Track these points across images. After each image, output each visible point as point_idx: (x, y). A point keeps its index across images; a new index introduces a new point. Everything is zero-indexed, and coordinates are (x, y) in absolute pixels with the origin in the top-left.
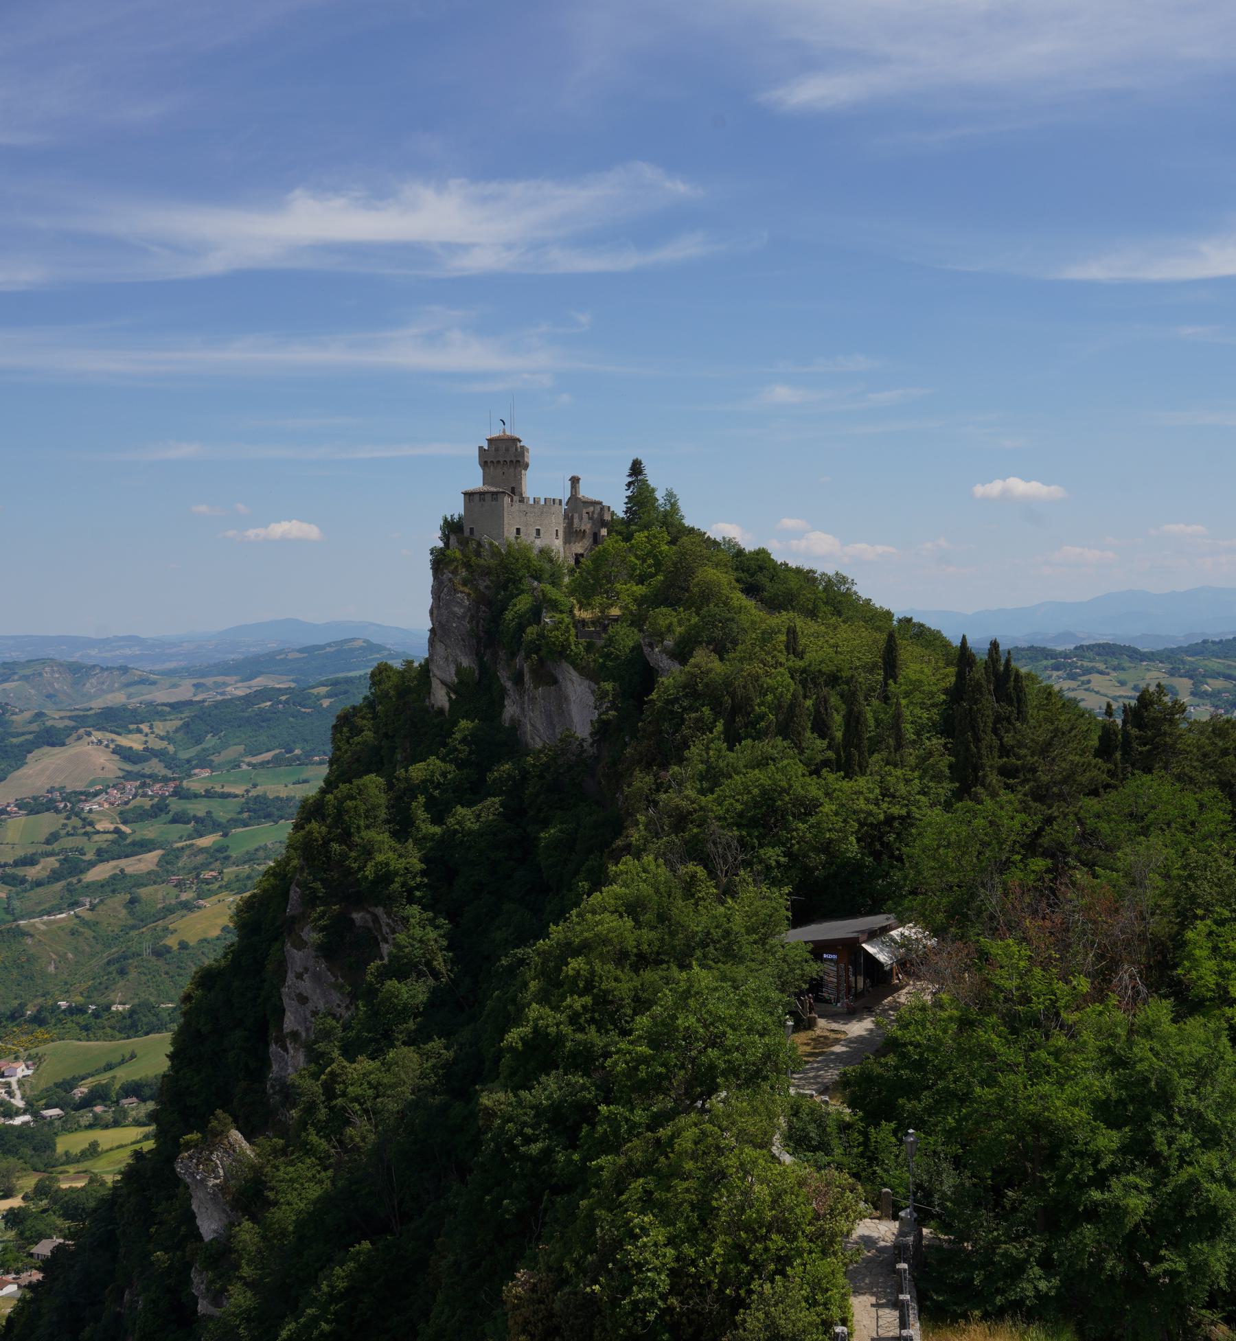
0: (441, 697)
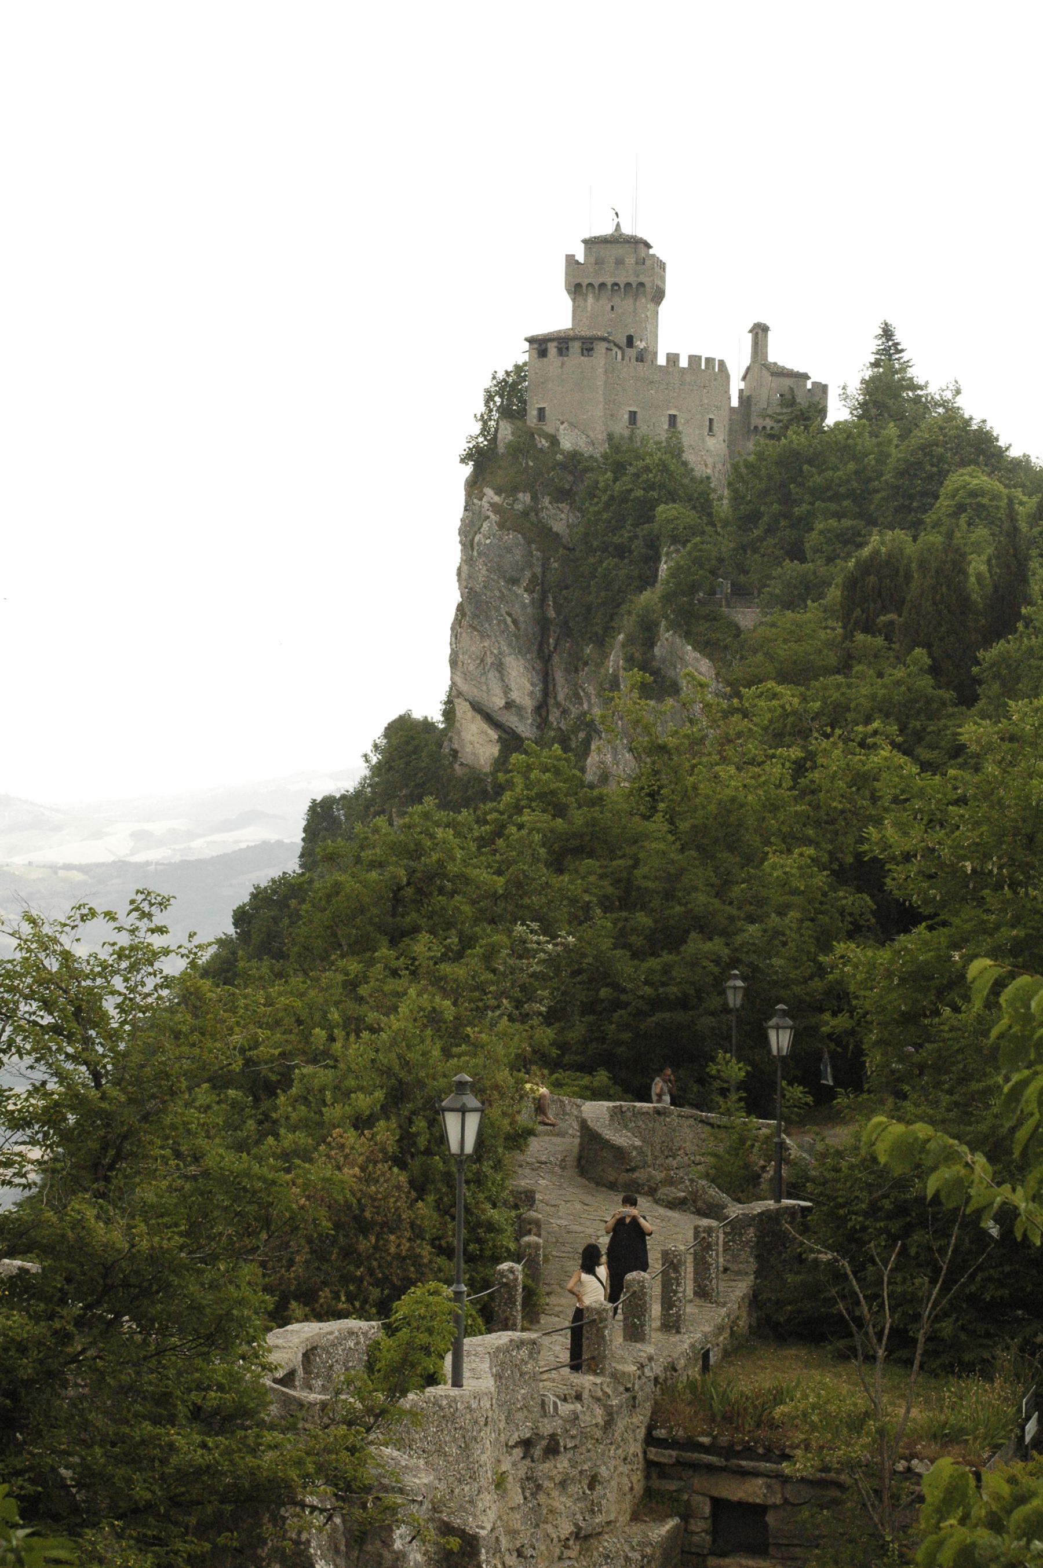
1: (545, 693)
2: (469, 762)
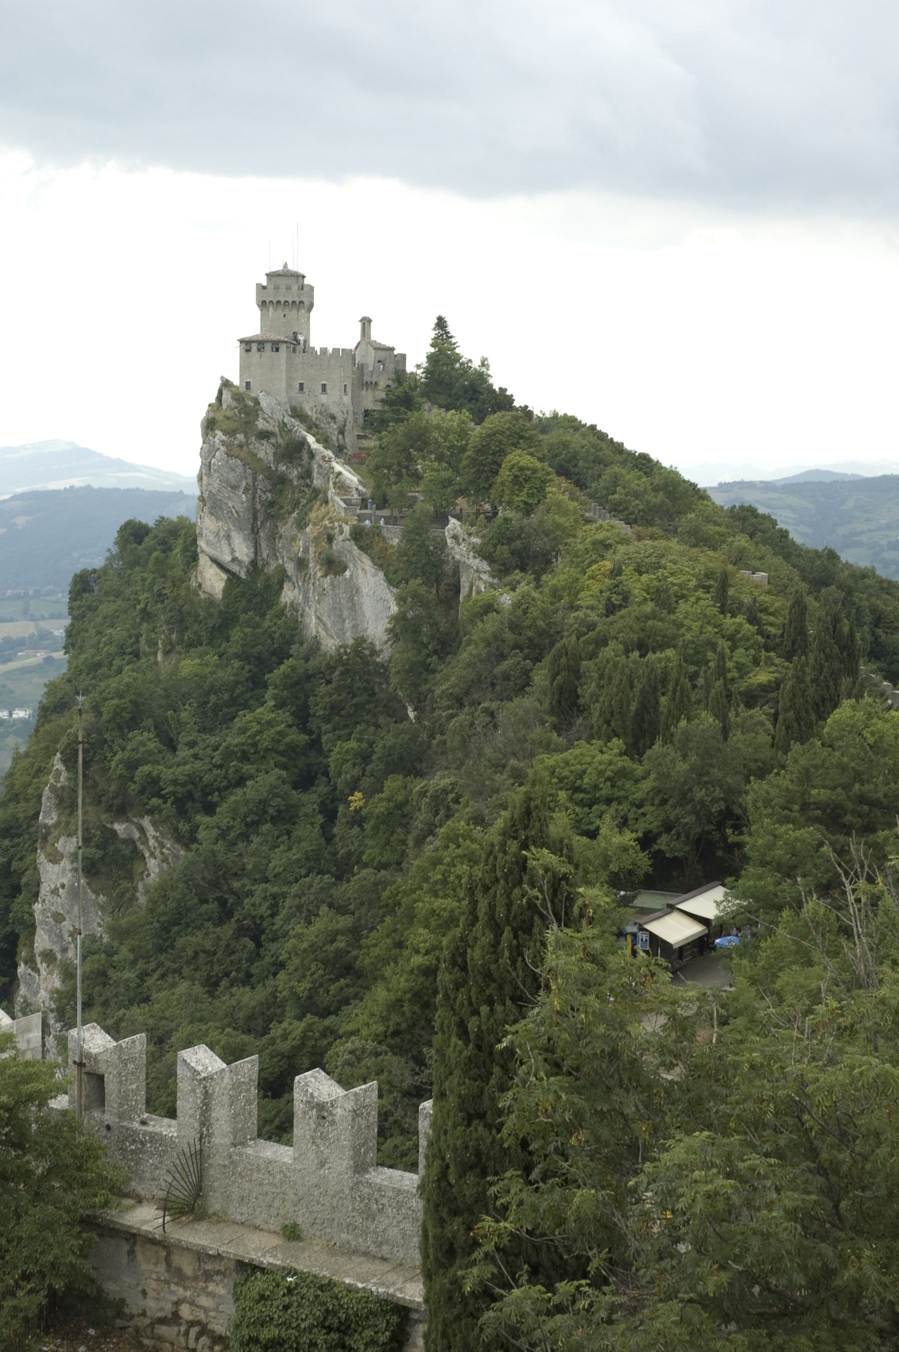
0: (213, 581)
1: (256, 553)
2: (209, 591)
